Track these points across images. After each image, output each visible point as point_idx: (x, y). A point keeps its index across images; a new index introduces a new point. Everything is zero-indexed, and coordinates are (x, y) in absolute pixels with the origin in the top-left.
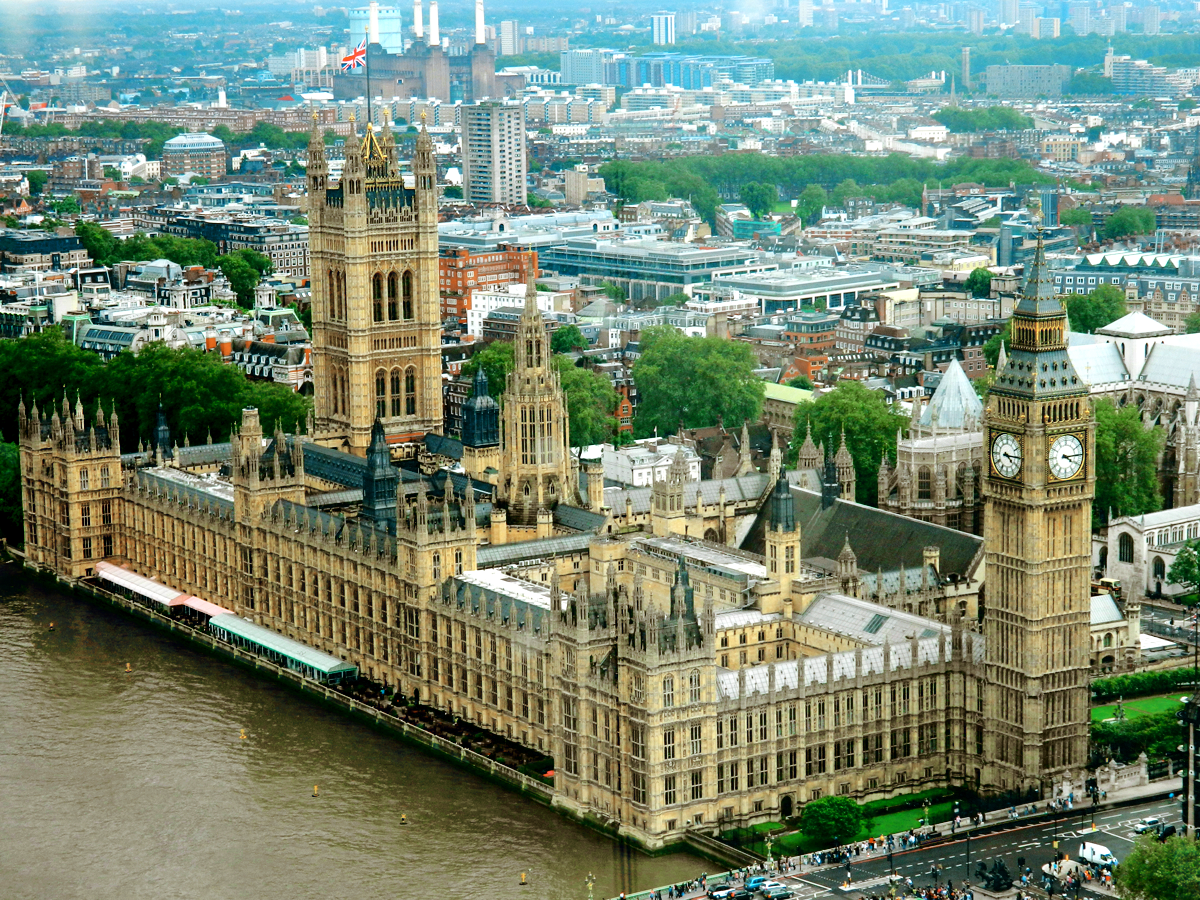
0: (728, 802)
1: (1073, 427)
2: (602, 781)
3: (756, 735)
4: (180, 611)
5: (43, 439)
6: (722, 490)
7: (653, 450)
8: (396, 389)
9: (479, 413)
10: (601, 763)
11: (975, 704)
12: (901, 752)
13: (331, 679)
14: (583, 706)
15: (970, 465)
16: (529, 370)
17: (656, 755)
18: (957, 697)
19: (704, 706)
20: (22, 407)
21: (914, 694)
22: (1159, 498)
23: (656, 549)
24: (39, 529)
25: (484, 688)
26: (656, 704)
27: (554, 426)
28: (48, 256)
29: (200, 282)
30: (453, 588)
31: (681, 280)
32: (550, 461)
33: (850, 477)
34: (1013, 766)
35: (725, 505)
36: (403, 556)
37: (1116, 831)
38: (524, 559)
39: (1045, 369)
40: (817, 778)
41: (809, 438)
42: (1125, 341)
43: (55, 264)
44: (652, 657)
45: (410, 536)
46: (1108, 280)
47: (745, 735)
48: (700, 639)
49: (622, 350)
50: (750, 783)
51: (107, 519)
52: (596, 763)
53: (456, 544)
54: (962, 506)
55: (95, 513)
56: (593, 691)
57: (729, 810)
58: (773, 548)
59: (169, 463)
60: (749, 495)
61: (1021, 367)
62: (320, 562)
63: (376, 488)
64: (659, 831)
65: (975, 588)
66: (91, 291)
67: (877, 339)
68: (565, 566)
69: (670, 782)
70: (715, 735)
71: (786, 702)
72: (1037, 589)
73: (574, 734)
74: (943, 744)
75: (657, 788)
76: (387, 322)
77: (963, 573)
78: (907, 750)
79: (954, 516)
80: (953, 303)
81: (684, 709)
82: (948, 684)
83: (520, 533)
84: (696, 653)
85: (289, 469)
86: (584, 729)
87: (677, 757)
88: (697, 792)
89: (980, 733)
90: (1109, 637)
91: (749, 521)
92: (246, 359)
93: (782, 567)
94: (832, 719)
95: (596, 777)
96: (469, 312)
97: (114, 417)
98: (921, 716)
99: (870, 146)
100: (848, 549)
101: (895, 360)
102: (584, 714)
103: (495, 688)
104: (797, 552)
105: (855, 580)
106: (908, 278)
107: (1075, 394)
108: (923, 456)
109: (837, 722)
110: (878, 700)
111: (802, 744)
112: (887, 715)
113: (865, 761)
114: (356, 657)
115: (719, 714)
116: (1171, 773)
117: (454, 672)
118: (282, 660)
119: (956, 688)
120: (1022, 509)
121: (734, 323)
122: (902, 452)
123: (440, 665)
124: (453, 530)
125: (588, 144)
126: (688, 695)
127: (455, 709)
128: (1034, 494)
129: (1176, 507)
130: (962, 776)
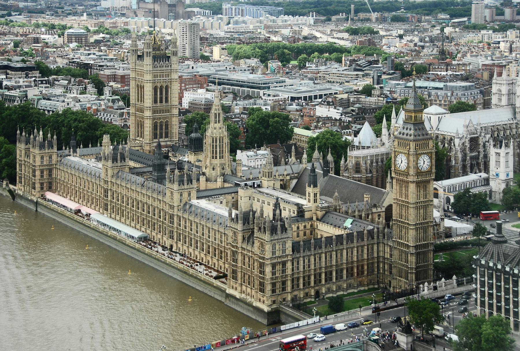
0: (296, 293)
3: (306, 267)
5: (26, 145)
6: (286, 170)
8: (161, 129)
9: (195, 140)
10: (247, 277)
11: (389, 255)
12: (360, 273)
20: (18, 132)
27: (224, 145)
29: (82, 85)
30: (188, 207)
31: (259, 88)
32: (222, 158)
33: (332, 165)
34: (404, 280)
35: (286, 175)
36: (168, 194)
38: (214, 195)
40: (329, 283)
41: (316, 152)
43: (27, 76)
44: (267, 237)
47: (302, 267)
48: (286, 229)
49: (239, 114)
50: (304, 285)
51: (50, 175)
52: (244, 276)
54: (372, 176)
57: (296, 296)
58: (309, 193)
59: (75, 155)
60: (295, 172)
62: (134, 195)
65: (384, 209)
66: (42, 87)
68: (229, 197)
69: (274, 285)
70: (291, 267)
73: (236, 265)
74: (376, 270)
76: (159, 104)
77: (378, 203)
78: (363, 273)
79: (369, 180)
81: (280, 257)
85: (123, 158)
86: (239, 265)
87: (277, 275)
88: (284, 289)
89: (391, 268)
91: (294, 182)
95: (244, 282)
97: (55, 137)
98: (368, 259)
99: (320, 40)
102: (240, 258)
103: (203, 246)
105: (339, 206)
106: (341, 89)
109: (337, 262)
110: (352, 253)
113: (347, 277)
115: (293, 259)
116: (465, 283)
119: (381, 249)
121: (280, 105)
122: (350, 156)
123: (181, 236)
124: (188, 184)
126: (281, 252)
127: (187, 253)
129: (452, 178)
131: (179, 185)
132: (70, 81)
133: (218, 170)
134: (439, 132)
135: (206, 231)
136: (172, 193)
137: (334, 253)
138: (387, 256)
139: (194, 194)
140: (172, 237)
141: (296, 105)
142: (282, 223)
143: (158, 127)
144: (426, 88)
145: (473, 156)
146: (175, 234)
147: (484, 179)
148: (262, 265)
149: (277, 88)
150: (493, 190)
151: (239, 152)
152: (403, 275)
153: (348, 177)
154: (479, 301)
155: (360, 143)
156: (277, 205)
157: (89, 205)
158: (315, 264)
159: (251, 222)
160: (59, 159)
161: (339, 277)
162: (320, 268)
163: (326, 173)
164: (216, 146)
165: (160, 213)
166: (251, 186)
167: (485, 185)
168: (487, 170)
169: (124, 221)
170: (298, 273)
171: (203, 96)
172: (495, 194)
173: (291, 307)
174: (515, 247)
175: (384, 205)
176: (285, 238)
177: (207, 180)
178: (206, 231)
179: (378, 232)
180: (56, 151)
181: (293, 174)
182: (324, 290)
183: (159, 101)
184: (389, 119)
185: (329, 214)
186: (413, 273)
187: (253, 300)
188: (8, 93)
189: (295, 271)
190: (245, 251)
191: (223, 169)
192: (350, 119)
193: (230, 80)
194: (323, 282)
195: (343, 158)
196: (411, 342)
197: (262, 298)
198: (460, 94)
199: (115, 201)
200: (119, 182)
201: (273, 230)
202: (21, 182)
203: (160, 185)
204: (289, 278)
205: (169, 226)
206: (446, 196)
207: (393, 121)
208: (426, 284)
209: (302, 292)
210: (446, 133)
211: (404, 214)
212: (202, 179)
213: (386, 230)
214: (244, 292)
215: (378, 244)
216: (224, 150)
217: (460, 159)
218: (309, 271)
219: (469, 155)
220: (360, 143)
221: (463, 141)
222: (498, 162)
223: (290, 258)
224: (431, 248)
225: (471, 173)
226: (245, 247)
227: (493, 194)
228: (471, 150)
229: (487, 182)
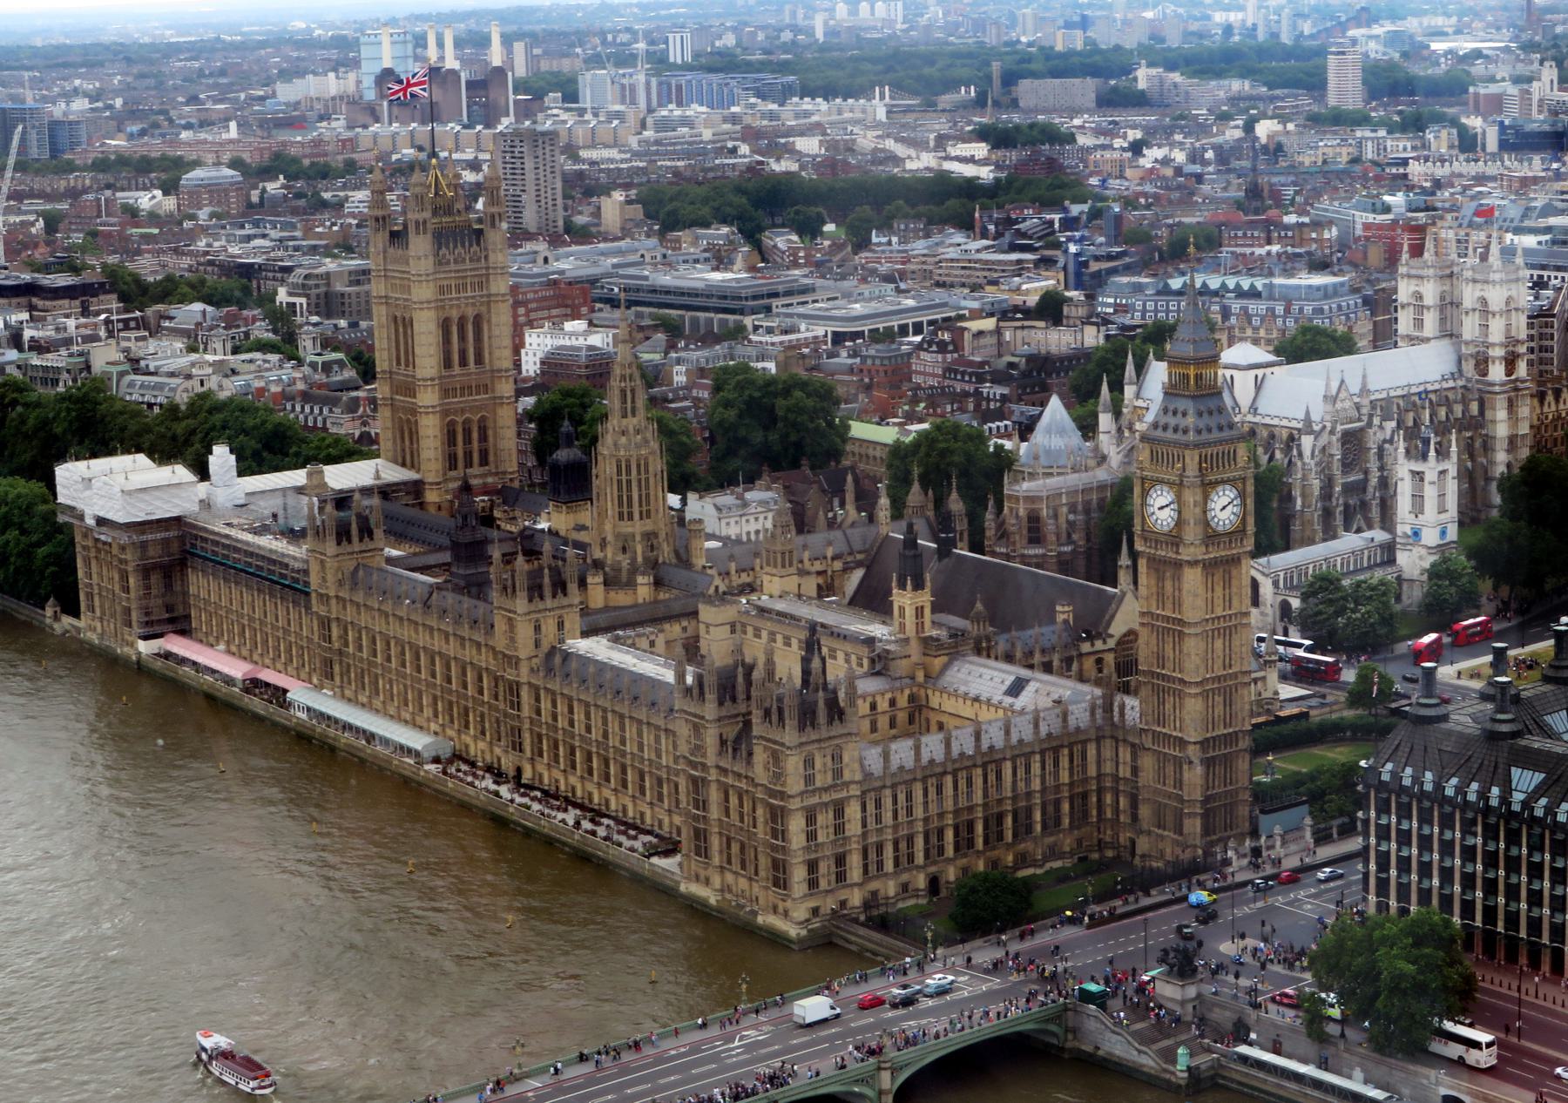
0: (874, 885)
2: (736, 866)
3: (902, 813)
6: (830, 543)
7: (740, 497)
8: (468, 440)
10: (735, 848)
11: (1129, 770)
12: (1053, 823)
14: (714, 787)
16: (625, 421)
18: (1109, 764)
19: (847, 784)
22: (1279, 542)
23: (769, 611)
24: (96, 599)
25: (595, 765)
26: (794, 784)
27: (652, 481)
28: (77, 302)
29: (238, 327)
30: (558, 659)
31: (742, 312)
32: (648, 516)
33: (961, 525)
35: (833, 559)
36: (500, 626)
37: (1287, 904)
39: (1200, 414)
40: (965, 856)
41: (916, 487)
42: (1235, 373)
43: (85, 312)
44: (790, 735)
45: (508, 604)
47: (890, 814)
50: (897, 863)
52: (729, 847)
53: (558, 612)
54: (1073, 551)
56: (724, 771)
57: (874, 894)
58: (902, 609)
63: (470, 552)
64: (802, 918)
66: (129, 339)
67: (956, 372)
68: (675, 630)
69: (812, 866)
70: (859, 816)
71: (931, 775)
72: (1193, 647)
74: (1094, 812)
75: (799, 874)
76: (457, 370)
78: (1058, 822)
81: (826, 789)
83: (621, 598)
84: (837, 729)
86: (715, 812)
87: (820, 839)
88: (841, 877)
91: (857, 575)
92: (298, 408)
94: (980, 793)
95: (729, 862)
96: (523, 352)
98: (1071, 784)
99: (910, 165)
100: (979, 606)
101: (977, 393)
102: (714, 795)
103: (607, 766)
104: (927, 611)
105: (988, 640)
106: (975, 305)
107: (1231, 441)
108: (1031, 499)
109: (986, 795)
110: (1028, 771)
114: (450, 732)
115: (864, 793)
117: (561, 749)
118: (370, 737)
119: (1108, 753)
120: (1178, 565)
121: (803, 356)
122: (1010, 497)
124: (554, 596)
125: (619, 170)
126: (830, 775)
127: (562, 787)
128: (1192, 549)
130: (1115, 845)
131: (530, 600)
134: (1257, 419)
135: (613, 726)
137: (979, 771)
139: (573, 621)
140: (518, 747)
141: (850, 356)
146: (527, 736)
147: (1381, 546)
148: (777, 816)
149: (790, 310)
150: (1406, 576)
152: (1170, 819)
154: (1372, 881)
156: (811, 646)
158: (926, 803)
159: (741, 696)
162: (941, 815)
163: (945, 549)
164: (629, 482)
165: (480, 679)
167: (1383, 564)
168: (1387, 521)
170: (880, 831)
171: (581, 342)
172: (1411, 588)
173: (862, 924)
175: (1111, 631)
176: (841, 736)
177: (606, 583)
178: (613, 726)
181: (850, 554)
184: (1117, 387)
186: (1195, 814)
188: (38, 363)
189: (871, 824)
190: (726, 776)
192: (1006, 391)
193: (654, 291)
194: (950, 851)
195: (991, 503)
196: (1193, 1000)
197: (781, 906)
198: (1308, 309)
199: (351, 650)
201: (807, 717)
203: (474, 602)
204: (855, 846)
206: (1280, 598)
207: (1129, 391)
208: (1231, 844)
210: (1275, 422)
212: (595, 580)
214: (730, 891)
216: (652, 493)
217: (1317, 492)
222: (1418, 501)
223: (855, 790)
224: (1245, 743)
225: (1347, 530)
226: (728, 766)
227: (1405, 586)
228: (1347, 466)
229: (1388, 553)
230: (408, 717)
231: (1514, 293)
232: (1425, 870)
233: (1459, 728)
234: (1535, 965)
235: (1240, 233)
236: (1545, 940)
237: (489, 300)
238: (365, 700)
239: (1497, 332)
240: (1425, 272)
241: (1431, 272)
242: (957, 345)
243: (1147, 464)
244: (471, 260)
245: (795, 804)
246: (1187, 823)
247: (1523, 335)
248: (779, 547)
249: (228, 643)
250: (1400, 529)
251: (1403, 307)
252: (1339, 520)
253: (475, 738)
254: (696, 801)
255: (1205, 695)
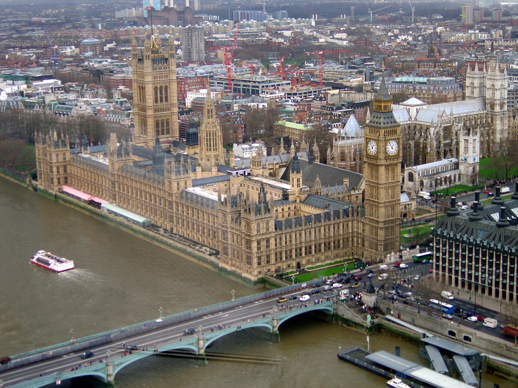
0: (279, 265)
1: (394, 138)
3: (288, 242)
4: (91, 202)
5: (43, 144)
6: (274, 159)
7: (250, 145)
8: (163, 126)
9: (191, 134)
10: (236, 252)
11: (362, 230)
13: (143, 225)
14: (229, 233)
15: (358, 150)
17: (255, 250)
19: (270, 233)
20: (36, 133)
21: (341, 227)
25: (195, 227)
27: (217, 139)
29: (94, 90)
30: (184, 194)
33: (317, 154)
34: (374, 251)
36: (167, 183)
40: (309, 256)
42: (410, 107)
44: (252, 217)
46: (403, 86)
47: (284, 242)
48: (269, 210)
49: (238, 111)
50: (286, 258)
51: (65, 171)
52: (234, 252)
55: (61, 169)
56: (232, 228)
57: (279, 267)
58: (293, 179)
59: (86, 152)
60: (283, 161)
61: (377, 118)
63: (158, 161)
65: (361, 192)
66: (58, 93)
67: (325, 107)
68: (222, 185)
69: (259, 258)
70: (274, 243)
72: (382, 192)
74: (351, 244)
76: (159, 103)
77: (357, 186)
80: (351, 94)
81: (263, 234)
82: (352, 224)
84: (268, 215)
86: (230, 242)
87: (262, 250)
88: (268, 262)
90: (406, 207)
91: (283, 170)
93: (295, 185)
94: (313, 237)
98: (343, 234)
100: (318, 179)
101: (331, 114)
102: (230, 236)
104: (301, 180)
105: (320, 190)
109: (315, 237)
110: (329, 230)
111: (304, 245)
112: (332, 235)
113: (324, 250)
114: (152, 217)
115: (276, 236)
119: (355, 225)
120: (378, 166)
121: (276, 101)
126: (265, 229)
128: (382, 161)
132: (83, 86)
133: (213, 161)
134: (417, 122)
136: (170, 182)
137: (313, 230)
138: (360, 231)
139: (190, 183)
142: (265, 205)
143: (160, 125)
144: (411, 82)
145: (447, 143)
146: (175, 218)
148: (249, 243)
150: (462, 173)
151: (235, 145)
153: (334, 165)
155: (346, 134)
156: (262, 189)
157: (100, 196)
160: (72, 156)
161: (318, 250)
164: (210, 139)
166: (242, 175)
167: (455, 169)
169: (130, 209)
174: (465, 218)
179: (353, 210)
180: (69, 149)
182: (304, 262)
183: (159, 101)
185: (310, 197)
186: (381, 245)
187: (242, 271)
191: (217, 160)
194: (303, 255)
198: (441, 88)
199: (121, 191)
200: (124, 174)
201: (258, 211)
202: (41, 178)
205: (169, 212)
206: (420, 179)
208: (393, 253)
209: (284, 264)
210: (422, 123)
211: (374, 194)
212: (199, 169)
213: (359, 209)
214: (234, 266)
215: (352, 221)
216: (217, 142)
217: (435, 146)
218: (291, 245)
219: (443, 142)
220: (346, 134)
221: (437, 130)
222: (466, 148)
223: (273, 235)
225: (444, 158)
227: (462, 177)
228: (445, 138)
229: (457, 166)
230: (139, 212)
231: (503, 83)
232: (444, 260)
233: (462, 217)
234: (483, 291)
235: (425, 64)
236: (480, 283)
237: (170, 81)
238: (126, 207)
239: (498, 95)
240: (475, 76)
241: (477, 76)
242: (326, 98)
243: (368, 134)
244: (164, 68)
245: (254, 239)
246: (379, 247)
247: (506, 97)
248: (257, 160)
249: (84, 189)
250: (460, 158)
251: (468, 87)
252: (442, 155)
253: (159, 219)
254: (224, 238)
255: (385, 207)
